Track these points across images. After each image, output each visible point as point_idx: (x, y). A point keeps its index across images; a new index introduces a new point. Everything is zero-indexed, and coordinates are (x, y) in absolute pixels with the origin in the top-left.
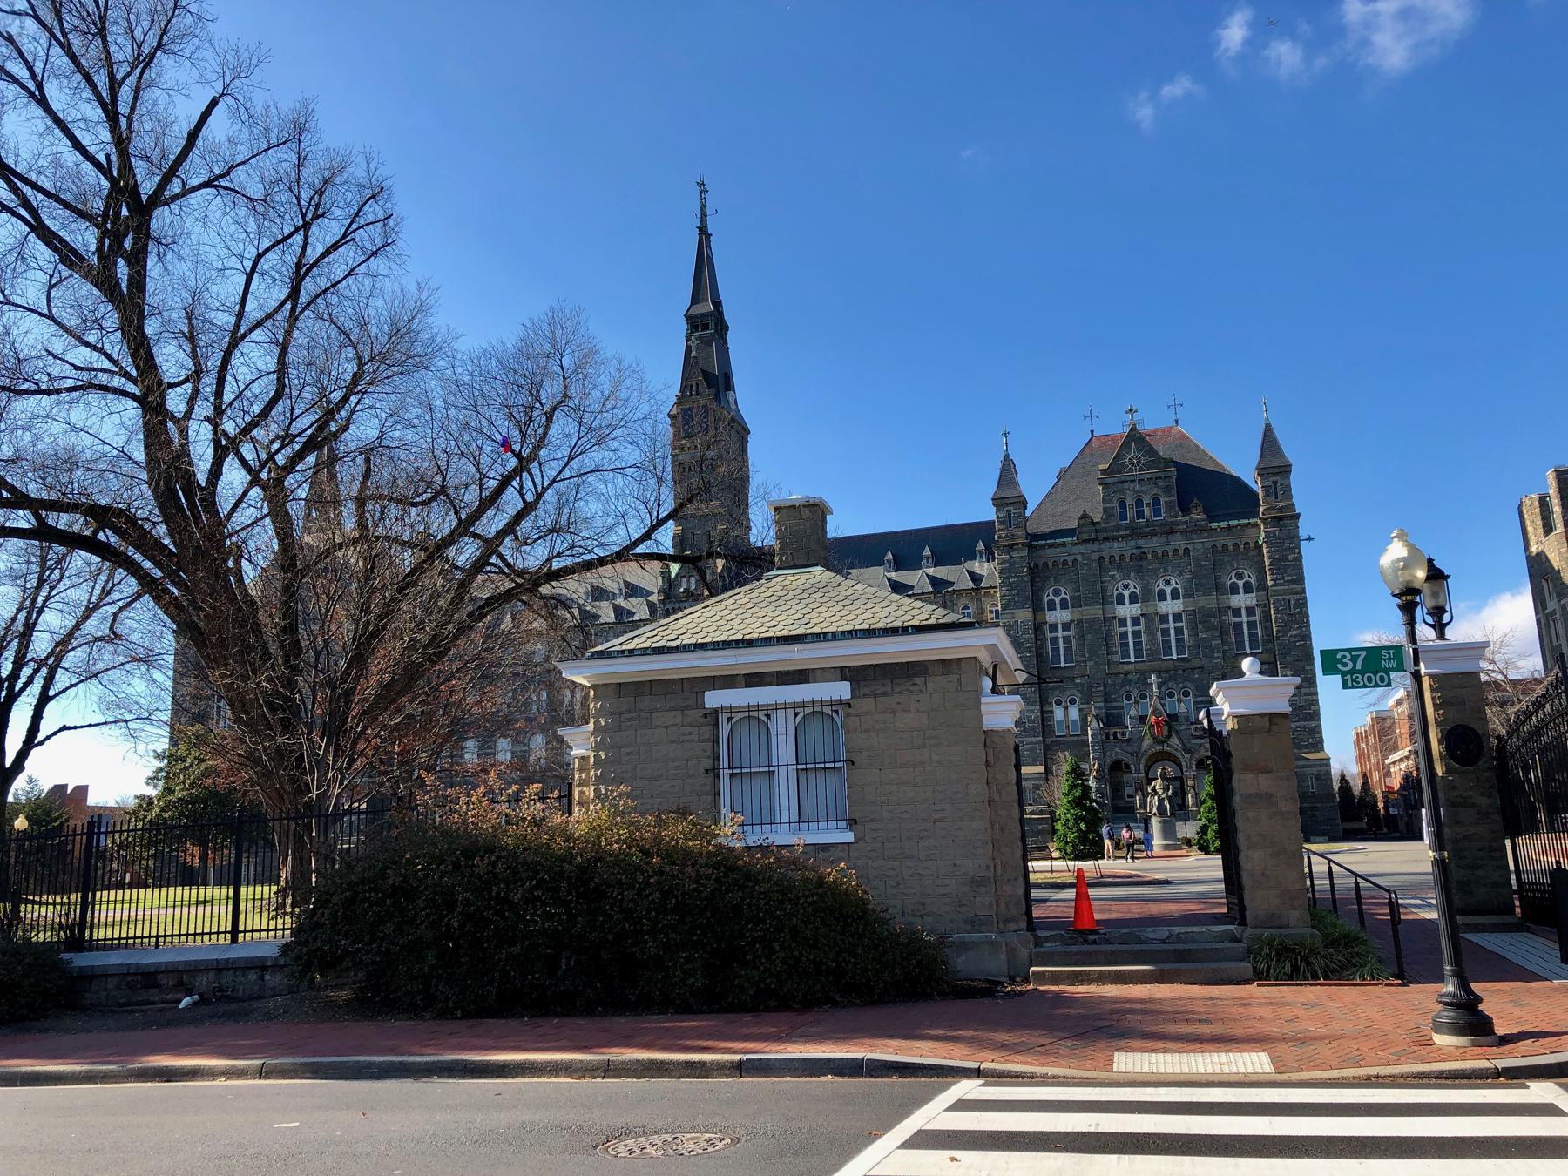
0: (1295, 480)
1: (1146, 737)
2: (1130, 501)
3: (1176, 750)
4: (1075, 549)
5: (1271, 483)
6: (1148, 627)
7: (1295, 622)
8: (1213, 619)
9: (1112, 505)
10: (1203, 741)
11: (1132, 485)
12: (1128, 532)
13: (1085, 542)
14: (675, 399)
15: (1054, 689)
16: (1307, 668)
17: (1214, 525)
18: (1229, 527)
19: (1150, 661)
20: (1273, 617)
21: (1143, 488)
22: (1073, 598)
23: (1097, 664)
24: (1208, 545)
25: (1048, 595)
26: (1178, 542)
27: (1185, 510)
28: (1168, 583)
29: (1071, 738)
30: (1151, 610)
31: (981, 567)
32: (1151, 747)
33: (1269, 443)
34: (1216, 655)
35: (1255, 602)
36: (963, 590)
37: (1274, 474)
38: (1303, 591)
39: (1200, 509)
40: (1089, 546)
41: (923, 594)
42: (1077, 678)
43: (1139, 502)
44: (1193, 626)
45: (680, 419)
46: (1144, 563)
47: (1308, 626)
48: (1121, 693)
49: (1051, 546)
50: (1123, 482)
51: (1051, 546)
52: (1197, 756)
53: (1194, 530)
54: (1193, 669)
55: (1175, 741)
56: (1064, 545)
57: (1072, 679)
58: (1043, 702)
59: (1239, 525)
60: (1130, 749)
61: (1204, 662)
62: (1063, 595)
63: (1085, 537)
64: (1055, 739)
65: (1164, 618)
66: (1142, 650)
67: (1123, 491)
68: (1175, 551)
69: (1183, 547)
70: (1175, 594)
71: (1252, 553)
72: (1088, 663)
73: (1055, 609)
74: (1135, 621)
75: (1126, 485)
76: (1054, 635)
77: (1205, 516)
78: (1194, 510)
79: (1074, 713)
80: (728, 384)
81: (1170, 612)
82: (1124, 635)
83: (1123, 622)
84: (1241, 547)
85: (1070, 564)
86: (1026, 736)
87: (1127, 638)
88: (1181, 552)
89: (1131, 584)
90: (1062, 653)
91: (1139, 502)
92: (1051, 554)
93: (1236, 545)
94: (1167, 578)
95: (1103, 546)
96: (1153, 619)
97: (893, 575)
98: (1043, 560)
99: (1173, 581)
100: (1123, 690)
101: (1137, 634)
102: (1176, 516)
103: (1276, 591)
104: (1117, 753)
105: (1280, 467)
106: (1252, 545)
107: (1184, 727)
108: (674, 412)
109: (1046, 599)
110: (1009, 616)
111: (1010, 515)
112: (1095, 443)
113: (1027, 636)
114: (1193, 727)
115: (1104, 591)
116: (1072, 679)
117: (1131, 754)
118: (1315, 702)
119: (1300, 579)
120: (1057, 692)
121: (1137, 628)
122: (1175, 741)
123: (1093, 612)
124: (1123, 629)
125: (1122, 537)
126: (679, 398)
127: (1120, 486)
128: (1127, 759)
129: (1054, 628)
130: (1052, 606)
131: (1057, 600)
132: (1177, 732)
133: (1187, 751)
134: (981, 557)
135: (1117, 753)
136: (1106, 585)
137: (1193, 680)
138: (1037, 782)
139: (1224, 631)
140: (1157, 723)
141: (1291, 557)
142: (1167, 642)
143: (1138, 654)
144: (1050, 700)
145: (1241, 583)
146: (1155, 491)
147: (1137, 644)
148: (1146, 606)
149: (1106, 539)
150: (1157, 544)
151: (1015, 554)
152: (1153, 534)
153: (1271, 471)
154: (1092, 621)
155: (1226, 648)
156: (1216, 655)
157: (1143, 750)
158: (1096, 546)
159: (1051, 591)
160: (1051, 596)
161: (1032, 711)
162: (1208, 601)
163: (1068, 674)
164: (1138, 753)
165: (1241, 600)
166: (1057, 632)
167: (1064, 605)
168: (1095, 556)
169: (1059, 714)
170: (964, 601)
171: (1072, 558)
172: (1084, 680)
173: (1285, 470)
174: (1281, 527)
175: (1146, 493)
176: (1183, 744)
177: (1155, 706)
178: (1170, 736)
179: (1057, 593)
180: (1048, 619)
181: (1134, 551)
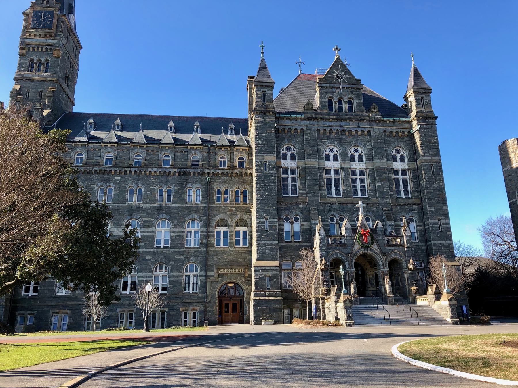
0: (433, 97)
1: (356, 243)
2: (336, 99)
3: (376, 253)
4: (303, 123)
5: (420, 98)
6: (345, 175)
7: (436, 180)
8: (384, 175)
9: (325, 100)
10: (393, 248)
11: (338, 90)
12: (335, 117)
13: (309, 119)
14: (30, 4)
15: (285, 209)
16: (444, 208)
17: (386, 119)
18: (394, 122)
19: (346, 197)
20: (424, 175)
21: (344, 93)
22: (300, 153)
23: (313, 195)
24: (382, 130)
25: (283, 150)
26: (364, 126)
27: (369, 110)
28: (356, 151)
29: (296, 244)
30: (346, 166)
31: (232, 137)
32: (359, 250)
33: (418, 78)
34: (386, 197)
35: (407, 167)
36: (223, 146)
37: (422, 93)
38: (440, 162)
39: (376, 109)
40: (311, 122)
41: (195, 145)
42: (300, 204)
43: (340, 102)
44: (372, 178)
45: (31, 16)
46: (344, 137)
47: (443, 183)
48: (328, 215)
49: (288, 119)
50: (333, 87)
51: (288, 119)
52: (389, 259)
53: (373, 121)
54: (373, 204)
55: (375, 247)
56: (295, 119)
57: (297, 204)
58: (280, 219)
59: (400, 121)
60: (345, 251)
61: (379, 200)
62: (292, 151)
63: (309, 116)
64: (284, 244)
65: (354, 172)
66: (339, 190)
67: (332, 93)
68: (363, 131)
69: (367, 130)
70: (360, 159)
71: (407, 139)
72: (308, 195)
73: (286, 159)
74: (336, 172)
75: (334, 90)
76: (285, 176)
77: (380, 114)
78: (373, 110)
79: (297, 227)
80: (71, 9)
81: (358, 168)
82: (329, 180)
83: (328, 172)
84: (400, 134)
85: (299, 131)
86: (268, 240)
87: (331, 182)
88: (366, 133)
89: (335, 149)
90: (290, 187)
91: (340, 102)
92: (287, 123)
93: (397, 132)
94: (356, 148)
95: (320, 123)
96: (348, 171)
97: (174, 135)
98: (282, 127)
99: (360, 149)
100: (330, 214)
101: (337, 180)
102: (362, 111)
103: (425, 160)
104: (337, 253)
105: (425, 89)
106: (406, 134)
107: (381, 238)
108: (28, 12)
109: (282, 153)
110: (261, 158)
111: (264, 94)
112: (302, 76)
113: (272, 172)
114: (386, 238)
115: (319, 151)
116: (297, 204)
117: (346, 254)
118: (449, 229)
119: (438, 155)
120: (287, 212)
121: (337, 176)
122: (375, 247)
123: (312, 163)
124: (328, 176)
125: (332, 119)
126: (33, 3)
127: (330, 90)
128: (343, 257)
129: (285, 171)
130: (285, 157)
131: (289, 154)
132: (377, 241)
133: (384, 254)
134: (231, 132)
135: (336, 253)
136: (320, 147)
137: (372, 211)
138: (274, 273)
139: (391, 184)
140: (364, 234)
141: (433, 141)
142: (355, 187)
143: (338, 192)
144: (282, 217)
145: (398, 156)
146: (351, 96)
147: (337, 187)
148: (344, 163)
149: (322, 119)
150: (351, 125)
151: (267, 118)
152: (351, 120)
153: (420, 91)
154: (311, 169)
155: (392, 193)
156: (386, 197)
157: (354, 252)
158: (315, 123)
159: (285, 148)
160: (285, 151)
161: (272, 222)
162: (382, 164)
163: (295, 201)
164: (351, 253)
165: (399, 166)
166: (287, 173)
167: (293, 157)
168: (315, 128)
169: (287, 227)
170: (222, 153)
171: (300, 128)
172: (305, 206)
173: (428, 91)
174: (427, 123)
175: (345, 96)
176: (381, 250)
177: (362, 222)
178: (372, 243)
179: (288, 149)
180: (282, 165)
181: (338, 128)
